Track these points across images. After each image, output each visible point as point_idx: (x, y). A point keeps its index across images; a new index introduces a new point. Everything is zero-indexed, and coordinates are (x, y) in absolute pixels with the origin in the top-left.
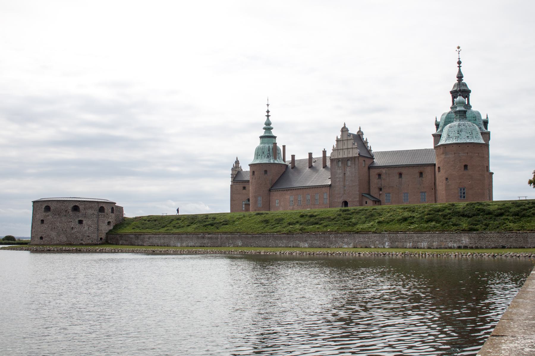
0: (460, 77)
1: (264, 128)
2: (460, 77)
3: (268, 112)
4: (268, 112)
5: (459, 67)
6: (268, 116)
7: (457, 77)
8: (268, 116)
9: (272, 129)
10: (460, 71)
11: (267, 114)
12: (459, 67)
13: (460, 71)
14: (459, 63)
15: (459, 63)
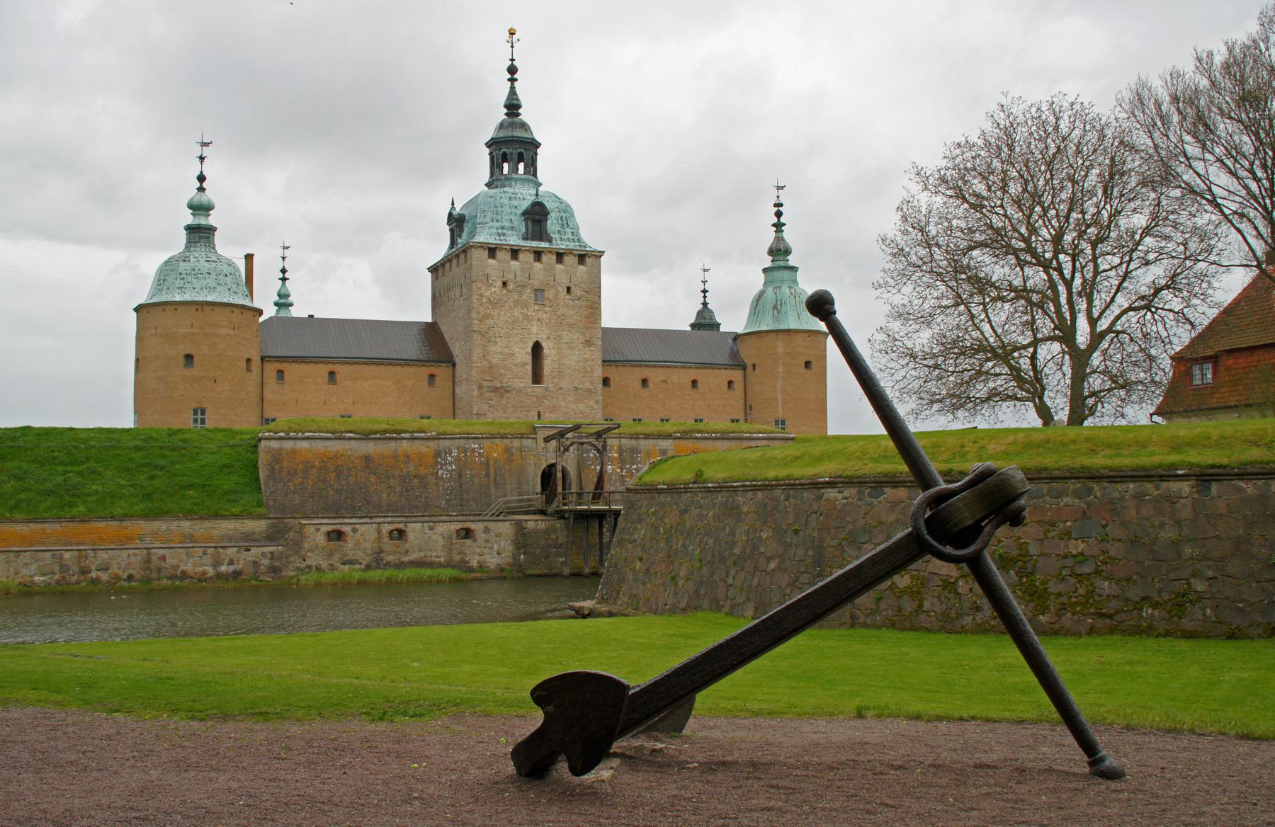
0: (513, 107)
1: (276, 304)
2: (513, 107)
3: (284, 271)
4: (284, 271)
5: (512, 80)
6: (284, 279)
7: (506, 106)
8: (284, 279)
9: (291, 305)
10: (513, 92)
11: (281, 275)
12: (512, 80)
13: (513, 92)
14: (512, 70)
15: (512, 70)
